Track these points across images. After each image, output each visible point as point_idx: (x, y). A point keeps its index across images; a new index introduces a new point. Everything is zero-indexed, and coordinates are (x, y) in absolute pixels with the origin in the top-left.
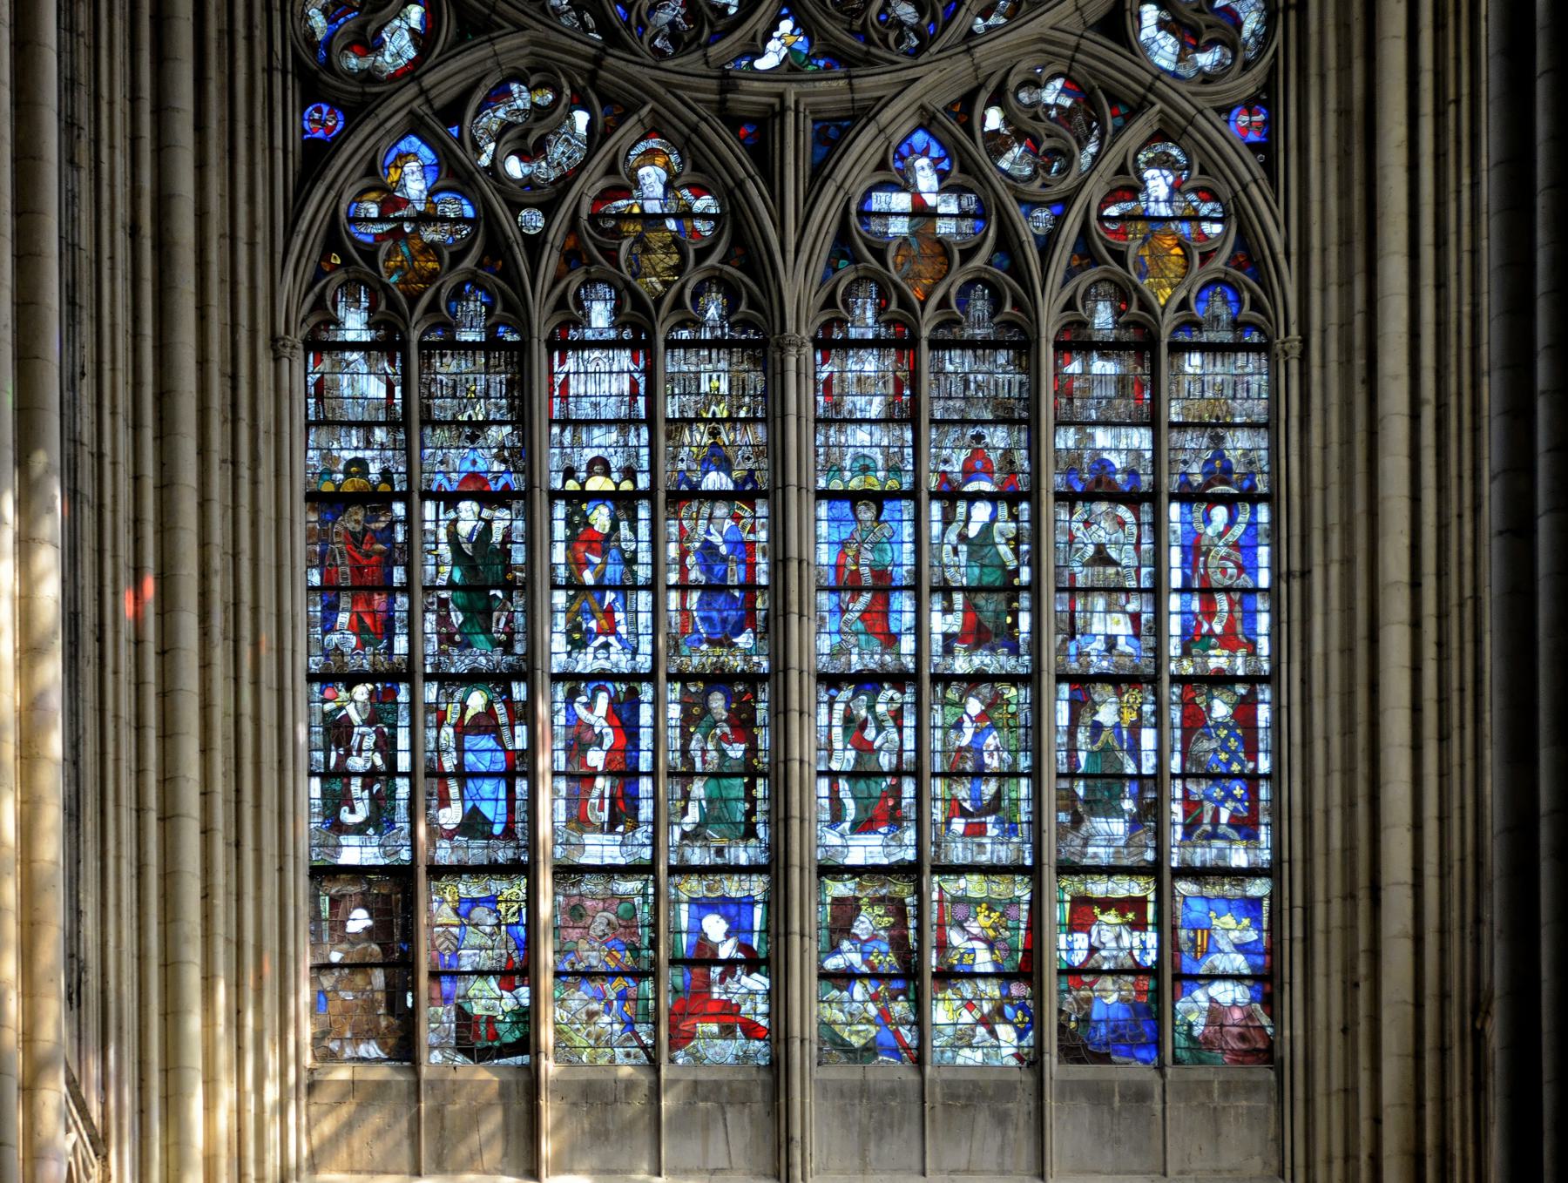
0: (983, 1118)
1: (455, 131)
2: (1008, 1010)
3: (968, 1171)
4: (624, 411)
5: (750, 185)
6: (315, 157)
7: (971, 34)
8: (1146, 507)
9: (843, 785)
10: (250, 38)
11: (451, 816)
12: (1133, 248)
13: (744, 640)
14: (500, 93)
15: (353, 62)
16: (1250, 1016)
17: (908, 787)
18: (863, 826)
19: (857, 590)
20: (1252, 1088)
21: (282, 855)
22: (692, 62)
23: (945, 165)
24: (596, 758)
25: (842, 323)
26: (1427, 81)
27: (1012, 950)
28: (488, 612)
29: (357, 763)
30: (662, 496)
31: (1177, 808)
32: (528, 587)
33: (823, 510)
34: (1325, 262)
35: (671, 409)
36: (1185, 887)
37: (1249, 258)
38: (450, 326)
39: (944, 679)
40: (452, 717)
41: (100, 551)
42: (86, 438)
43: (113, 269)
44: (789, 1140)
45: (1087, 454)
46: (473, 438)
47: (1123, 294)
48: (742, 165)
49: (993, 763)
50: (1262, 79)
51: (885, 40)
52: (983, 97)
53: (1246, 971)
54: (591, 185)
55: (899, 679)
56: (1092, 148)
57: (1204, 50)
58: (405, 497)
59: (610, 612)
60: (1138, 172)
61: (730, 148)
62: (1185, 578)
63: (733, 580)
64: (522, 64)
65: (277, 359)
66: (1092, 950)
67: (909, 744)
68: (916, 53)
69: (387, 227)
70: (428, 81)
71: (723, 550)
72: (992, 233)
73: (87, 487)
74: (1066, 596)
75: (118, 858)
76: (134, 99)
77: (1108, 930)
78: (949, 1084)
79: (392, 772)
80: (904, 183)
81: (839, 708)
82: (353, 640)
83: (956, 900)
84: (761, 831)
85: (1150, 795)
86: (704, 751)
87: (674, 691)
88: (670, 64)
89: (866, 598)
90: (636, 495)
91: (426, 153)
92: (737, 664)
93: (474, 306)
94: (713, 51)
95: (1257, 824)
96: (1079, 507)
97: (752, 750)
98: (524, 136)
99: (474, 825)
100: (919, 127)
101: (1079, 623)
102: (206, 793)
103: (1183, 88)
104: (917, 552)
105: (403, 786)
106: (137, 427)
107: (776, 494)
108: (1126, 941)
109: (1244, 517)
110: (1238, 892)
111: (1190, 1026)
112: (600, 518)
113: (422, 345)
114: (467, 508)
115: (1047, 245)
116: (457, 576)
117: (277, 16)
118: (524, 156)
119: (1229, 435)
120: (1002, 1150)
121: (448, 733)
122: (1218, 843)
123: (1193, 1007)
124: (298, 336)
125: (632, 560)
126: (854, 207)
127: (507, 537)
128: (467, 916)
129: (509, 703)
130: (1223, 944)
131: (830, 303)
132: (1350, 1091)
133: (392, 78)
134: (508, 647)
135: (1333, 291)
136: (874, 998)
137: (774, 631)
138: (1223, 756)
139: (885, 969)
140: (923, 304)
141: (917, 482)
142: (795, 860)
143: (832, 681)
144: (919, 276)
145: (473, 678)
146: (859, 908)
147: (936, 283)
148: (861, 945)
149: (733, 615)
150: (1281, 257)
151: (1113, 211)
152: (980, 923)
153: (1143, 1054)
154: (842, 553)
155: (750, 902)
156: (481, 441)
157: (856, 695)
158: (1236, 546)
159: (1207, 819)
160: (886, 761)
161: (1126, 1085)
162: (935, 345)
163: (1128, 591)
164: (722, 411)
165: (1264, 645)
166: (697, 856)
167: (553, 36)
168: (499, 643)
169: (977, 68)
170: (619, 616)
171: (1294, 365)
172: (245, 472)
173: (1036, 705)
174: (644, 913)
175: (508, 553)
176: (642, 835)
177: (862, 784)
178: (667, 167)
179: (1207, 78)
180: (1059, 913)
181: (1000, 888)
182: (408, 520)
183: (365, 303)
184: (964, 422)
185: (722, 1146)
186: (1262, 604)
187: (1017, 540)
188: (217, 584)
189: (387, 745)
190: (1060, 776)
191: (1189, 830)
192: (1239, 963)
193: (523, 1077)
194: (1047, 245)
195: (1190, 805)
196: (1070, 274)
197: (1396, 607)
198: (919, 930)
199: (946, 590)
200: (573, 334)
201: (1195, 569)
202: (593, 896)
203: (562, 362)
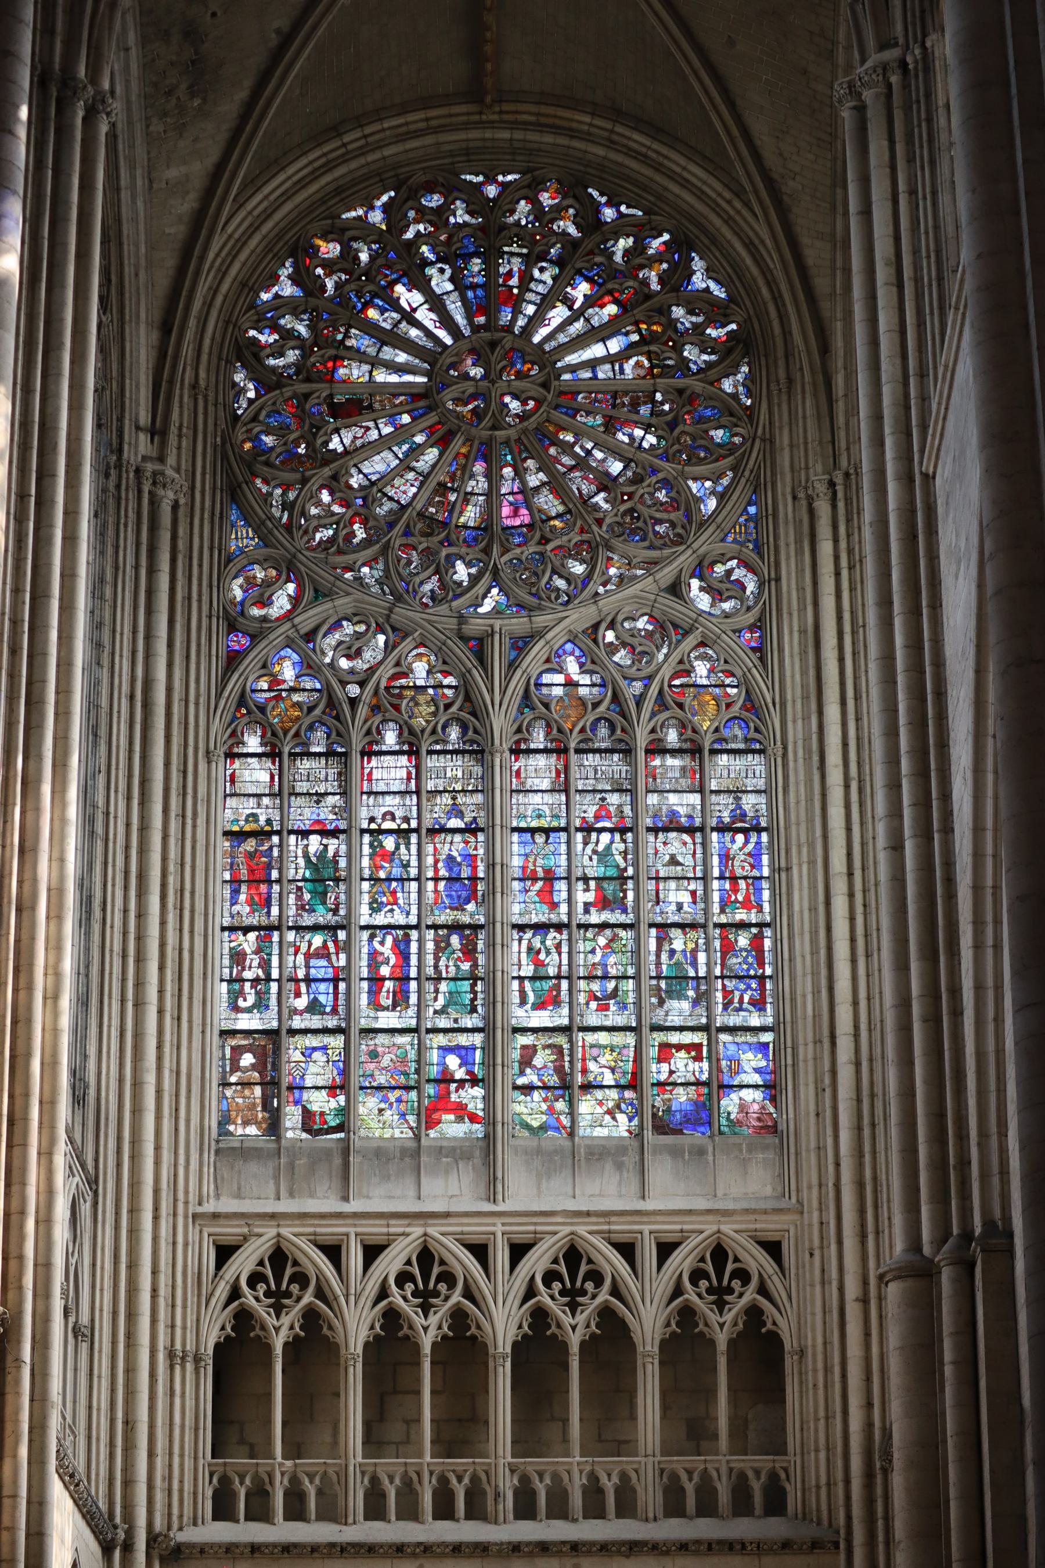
0: (609, 1166)
1: (311, 645)
2: (623, 1106)
3: (600, 1195)
4: (403, 788)
5: (474, 671)
6: (233, 659)
7: (597, 594)
8: (698, 835)
9: (527, 983)
10: (200, 601)
11: (302, 1003)
12: (687, 701)
13: (471, 907)
14: (337, 625)
15: (256, 612)
16: (763, 1108)
17: (564, 984)
18: (539, 1006)
19: (535, 879)
20: (766, 1148)
21: (204, 1024)
22: (443, 609)
23: (583, 660)
24: (385, 971)
25: (526, 740)
26: (847, 616)
27: (624, 1073)
28: (325, 893)
29: (248, 975)
30: (424, 831)
31: (719, 995)
32: (347, 880)
33: (515, 837)
34: (795, 708)
35: (430, 785)
36: (724, 1037)
37: (753, 706)
38: (306, 744)
39: (586, 927)
40: (304, 948)
41: (106, 863)
42: (100, 805)
43: (119, 717)
44: (495, 1179)
45: (664, 808)
46: (318, 802)
47: (682, 726)
48: (469, 661)
49: (613, 971)
50: (757, 615)
51: (549, 598)
52: (604, 625)
53: (761, 1083)
54: (386, 672)
55: (559, 927)
56: (665, 650)
57: (725, 601)
58: (279, 833)
59: (394, 893)
60: (690, 661)
62: (721, 871)
63: (464, 875)
64: (349, 611)
65: (209, 762)
66: (671, 1072)
67: (565, 961)
68: (568, 602)
69: (273, 694)
70: (297, 620)
71: (459, 859)
72: (609, 694)
73: (100, 829)
74: (654, 882)
75: (109, 1026)
76: (135, 632)
77: (681, 1060)
78: (588, 1147)
79: (268, 979)
81: (525, 943)
82: (248, 909)
83: (592, 1046)
84: (479, 1009)
85: (703, 988)
86: (447, 967)
87: (430, 934)
88: (430, 611)
89: (540, 884)
90: (410, 831)
91: (295, 657)
92: (466, 919)
93: (320, 734)
94: (455, 604)
95: (765, 1003)
96: (660, 835)
97: (475, 966)
98: (349, 648)
99: (314, 1007)
100: (569, 641)
101: (661, 896)
102: (161, 992)
103: (714, 620)
104: (569, 859)
105: (274, 987)
106: (129, 798)
107: (488, 829)
108: (691, 1067)
109: (754, 839)
110: (755, 1040)
111: (729, 1114)
112: (389, 843)
113: (290, 754)
114: (314, 840)
115: (639, 701)
116: (308, 874)
117: (215, 590)
118: (349, 657)
119: (744, 797)
120: (620, 1184)
121: (300, 958)
122: (742, 1013)
123: (730, 1103)
124: (221, 751)
125: (406, 866)
126: (532, 682)
127: (336, 854)
128: (310, 1056)
129: (336, 942)
130: (747, 1068)
131: (519, 730)
133: (277, 619)
134: (335, 912)
135: (800, 722)
136: (545, 1100)
137: (488, 901)
138: (745, 967)
139: (552, 1084)
140: (571, 731)
141: (568, 823)
142: (499, 1024)
143: (521, 928)
144: (569, 716)
145: (315, 928)
146: (536, 1051)
147: (579, 719)
148: (538, 1070)
149: (464, 894)
150: (770, 705)
151: (677, 682)
152: (606, 1058)
153: (702, 1129)
154: (527, 860)
155: (474, 1048)
156: (323, 804)
157: (534, 935)
158: (749, 854)
159: (736, 1000)
160: (552, 971)
161: (692, 1146)
162: (578, 751)
163: (689, 879)
164: (459, 787)
165: (766, 907)
166: (443, 1023)
167: (366, 597)
168: (331, 910)
169: (600, 611)
170: (399, 895)
171: (779, 761)
172: (189, 821)
173: (637, 940)
174: (412, 1055)
175: (337, 862)
176: (412, 1011)
177: (538, 984)
178: (429, 662)
179: (727, 615)
181: (618, 1039)
182: (280, 845)
183: (259, 733)
184: (594, 791)
185: (456, 1182)
186: (765, 885)
187: (625, 853)
188: (171, 879)
189: (266, 965)
190: (651, 978)
191: (726, 1007)
192: (757, 1079)
193: (341, 1145)
194: (639, 701)
195: (727, 993)
196: (653, 714)
197: (840, 886)
198: (571, 1062)
199: (585, 879)
200: (375, 748)
201: (726, 867)
202: (383, 1046)
203: (369, 762)
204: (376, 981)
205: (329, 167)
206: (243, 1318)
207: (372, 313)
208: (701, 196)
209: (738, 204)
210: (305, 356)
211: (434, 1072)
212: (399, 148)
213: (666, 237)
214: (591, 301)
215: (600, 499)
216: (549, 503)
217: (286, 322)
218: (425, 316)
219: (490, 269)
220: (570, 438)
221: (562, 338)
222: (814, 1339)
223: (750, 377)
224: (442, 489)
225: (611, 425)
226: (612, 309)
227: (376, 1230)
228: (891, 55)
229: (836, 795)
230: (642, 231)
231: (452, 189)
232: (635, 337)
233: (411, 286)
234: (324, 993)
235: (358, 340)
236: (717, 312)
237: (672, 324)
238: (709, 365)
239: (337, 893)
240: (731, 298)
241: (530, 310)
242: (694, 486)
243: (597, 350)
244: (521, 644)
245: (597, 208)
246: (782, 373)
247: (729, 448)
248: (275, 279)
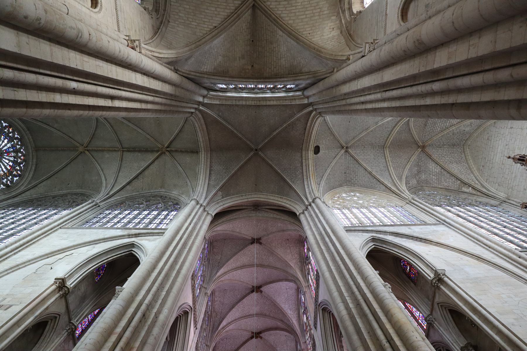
205: (23, 129)
209: (28, 182)
212: (27, 138)
213: (20, 173)
214: (10, 166)
218: (4, 144)
221: (4, 162)
223: (4, 188)
226: (9, 168)
230: (20, 170)
232: (6, 172)
233: (8, 142)
236: (12, 182)
237: (9, 177)
238: (4, 182)
240: (14, 183)
241: (7, 158)
243: (3, 167)
246: (6, 193)
248: (5, 123)
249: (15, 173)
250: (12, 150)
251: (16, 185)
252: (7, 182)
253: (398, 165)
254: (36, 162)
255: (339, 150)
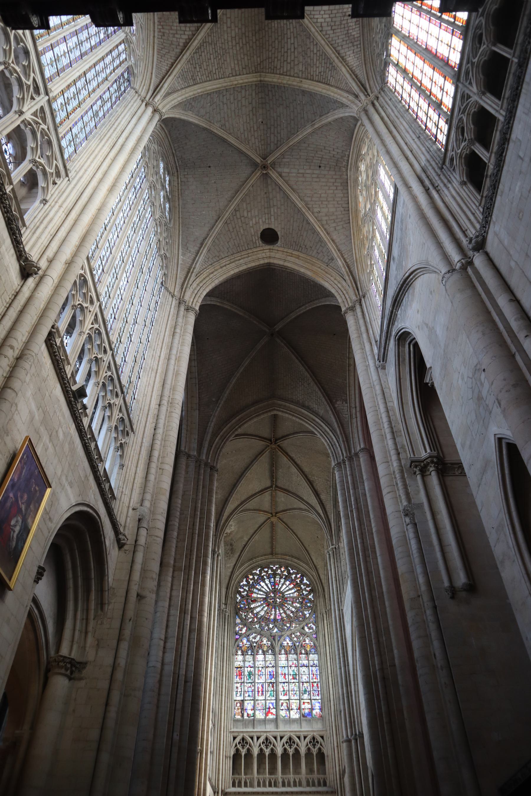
6: (237, 639)
11: (247, 695)
13: (273, 679)
15: (240, 632)
18: (284, 695)
19: (283, 674)
36: (313, 701)
47: (305, 650)
48: (272, 640)
61: (271, 639)
80: (286, 641)
99: (249, 696)
107: (276, 667)
112: (260, 669)
132: (329, 720)
137: (276, 678)
166: (269, 698)
180: (302, 703)
189: (241, 689)
194: (298, 646)
197: (330, 675)
204: (258, 692)
205: (251, 565)
206: (237, 750)
207: (257, 587)
208: (305, 568)
210: (248, 592)
211: (268, 707)
214: (289, 584)
215: (291, 615)
216: (284, 615)
217: (245, 588)
218: (265, 587)
219: (275, 580)
220: (286, 605)
222: (330, 753)
224: (268, 613)
225: (293, 603)
226: (292, 586)
227: (259, 734)
228: (334, 546)
229: (329, 661)
230: (296, 574)
231: (269, 568)
234: (250, 694)
235: (255, 590)
237: (301, 588)
239: (252, 677)
241: (280, 586)
242: (305, 612)
243: (290, 592)
244: (280, 637)
245: (290, 570)
247: (310, 607)
248: (243, 581)
249: (298, 581)
250: (272, 579)
251: (313, 582)
252: (306, 591)
253: (300, 50)
254: (289, 556)
255: (269, 181)
